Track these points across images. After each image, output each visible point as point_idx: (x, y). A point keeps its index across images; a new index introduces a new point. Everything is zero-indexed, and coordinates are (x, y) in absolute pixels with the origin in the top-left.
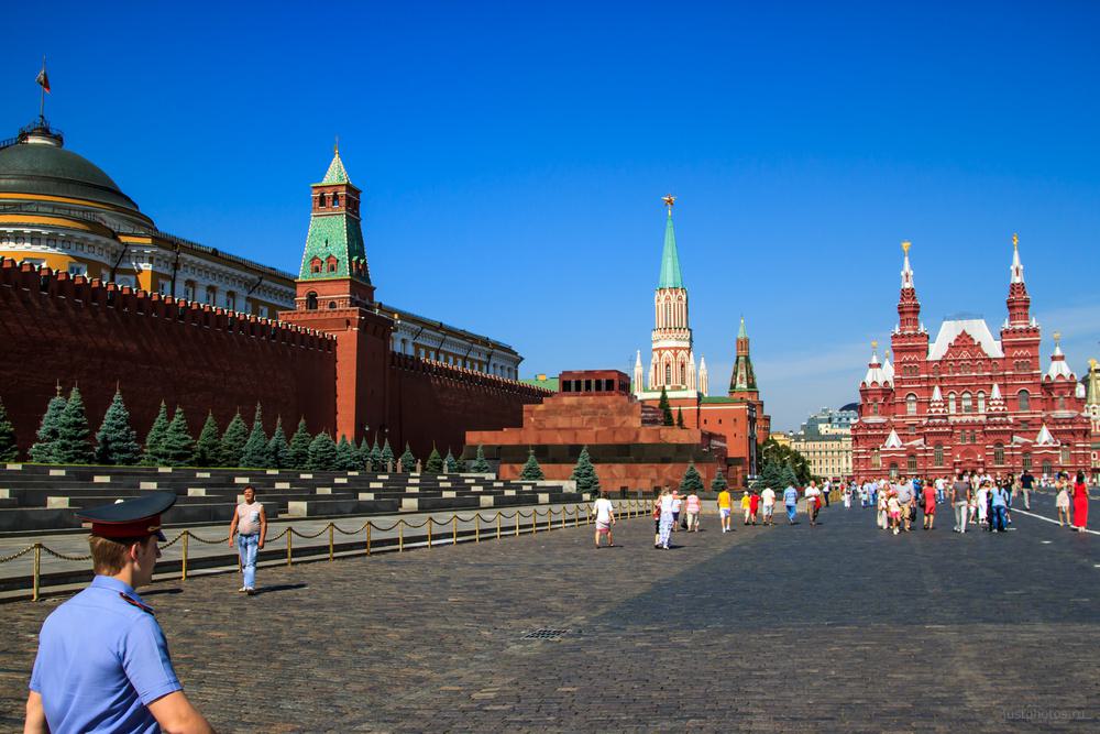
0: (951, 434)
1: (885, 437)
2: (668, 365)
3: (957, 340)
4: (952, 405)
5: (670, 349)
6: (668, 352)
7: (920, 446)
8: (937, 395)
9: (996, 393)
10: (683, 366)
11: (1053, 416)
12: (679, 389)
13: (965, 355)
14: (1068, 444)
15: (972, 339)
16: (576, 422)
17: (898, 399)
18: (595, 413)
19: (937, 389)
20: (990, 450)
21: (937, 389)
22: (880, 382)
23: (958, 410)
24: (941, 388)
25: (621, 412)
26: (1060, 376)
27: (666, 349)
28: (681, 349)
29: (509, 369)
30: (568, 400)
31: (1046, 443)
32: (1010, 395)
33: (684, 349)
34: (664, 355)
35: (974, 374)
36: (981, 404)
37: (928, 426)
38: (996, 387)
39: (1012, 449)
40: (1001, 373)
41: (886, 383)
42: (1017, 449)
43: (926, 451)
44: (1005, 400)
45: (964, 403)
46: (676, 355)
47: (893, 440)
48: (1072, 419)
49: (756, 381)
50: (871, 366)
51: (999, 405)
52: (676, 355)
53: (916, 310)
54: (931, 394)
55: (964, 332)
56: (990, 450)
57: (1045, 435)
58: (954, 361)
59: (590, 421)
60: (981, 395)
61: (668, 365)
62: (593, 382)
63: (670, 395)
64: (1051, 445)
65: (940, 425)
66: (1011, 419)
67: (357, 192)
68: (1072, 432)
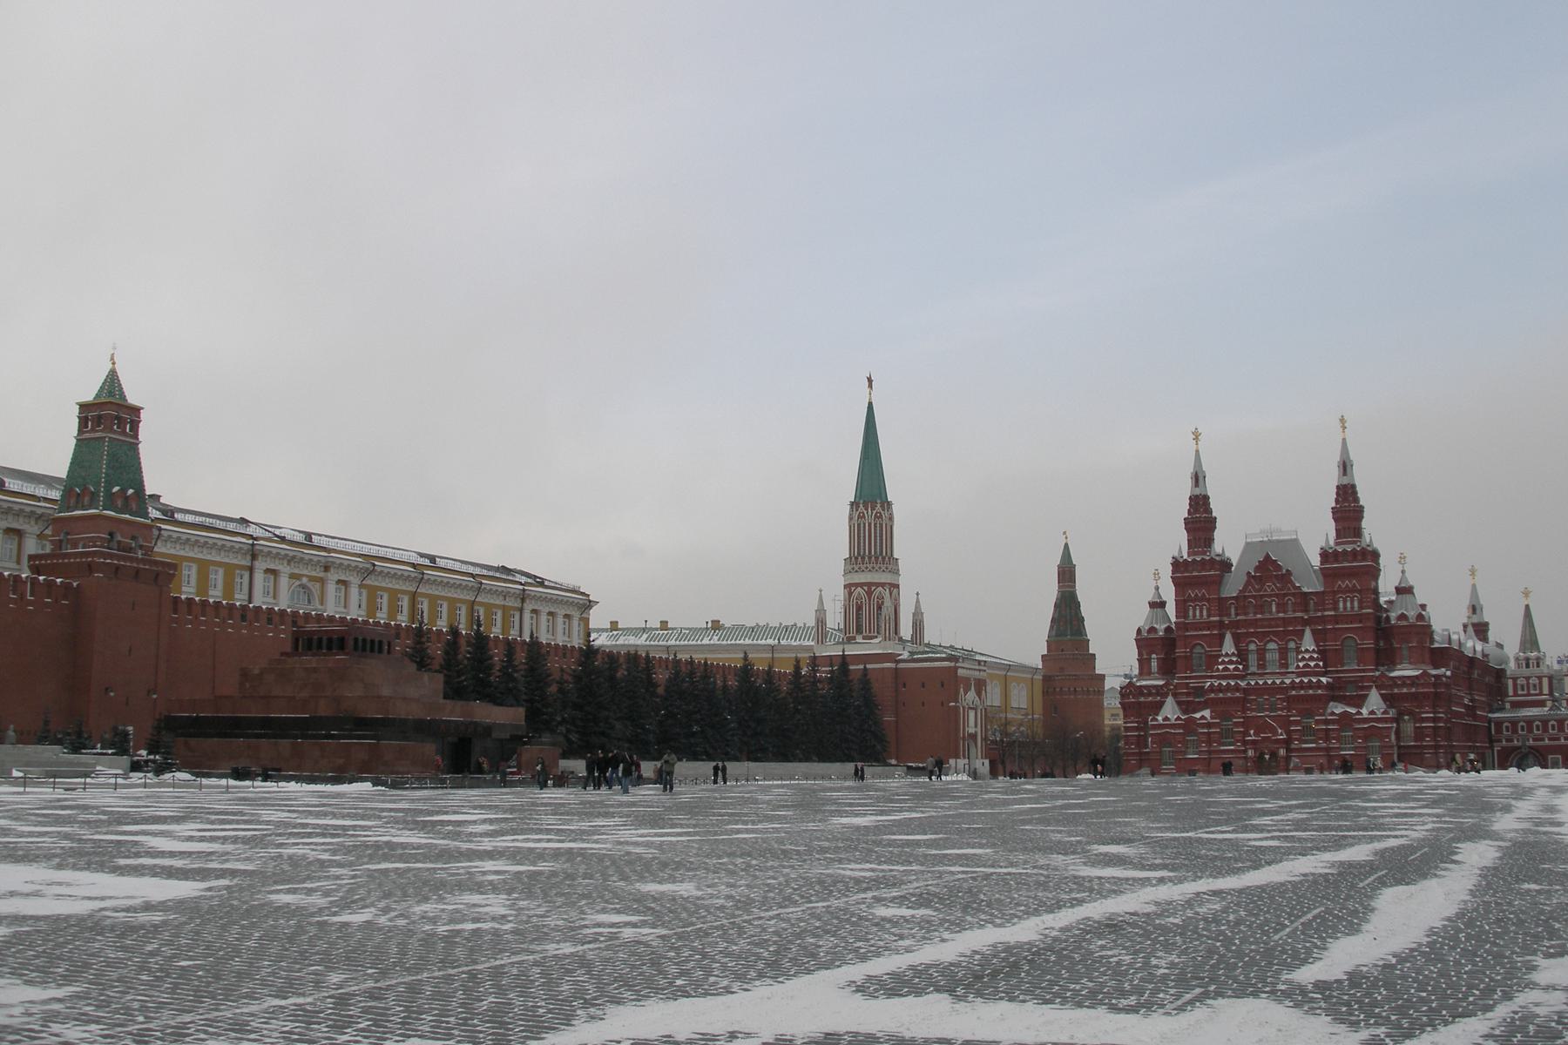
0: (1245, 700)
2: (859, 608)
3: (1257, 569)
4: (1253, 659)
5: (861, 585)
7: (1203, 717)
8: (1229, 646)
9: (1308, 643)
10: (880, 608)
13: (1269, 587)
14: (1410, 713)
15: (1279, 568)
17: (1180, 651)
19: (1228, 638)
20: (1297, 723)
21: (1228, 638)
22: (1161, 628)
24: (1237, 639)
27: (857, 585)
28: (878, 585)
29: (567, 616)
31: (1372, 712)
32: (1331, 645)
33: (883, 585)
34: (855, 594)
36: (1292, 655)
38: (1308, 634)
39: (1327, 722)
41: (1168, 629)
42: (1333, 722)
43: (1209, 725)
44: (1323, 654)
46: (869, 593)
47: (1170, 711)
48: (1416, 677)
50: (1153, 605)
51: (1311, 659)
52: (869, 593)
53: (1210, 524)
54: (1221, 645)
56: (1297, 723)
57: (1374, 703)
58: (1254, 597)
60: (1292, 645)
61: (859, 608)
66: (1324, 680)
67: (136, 410)
68: (1414, 697)
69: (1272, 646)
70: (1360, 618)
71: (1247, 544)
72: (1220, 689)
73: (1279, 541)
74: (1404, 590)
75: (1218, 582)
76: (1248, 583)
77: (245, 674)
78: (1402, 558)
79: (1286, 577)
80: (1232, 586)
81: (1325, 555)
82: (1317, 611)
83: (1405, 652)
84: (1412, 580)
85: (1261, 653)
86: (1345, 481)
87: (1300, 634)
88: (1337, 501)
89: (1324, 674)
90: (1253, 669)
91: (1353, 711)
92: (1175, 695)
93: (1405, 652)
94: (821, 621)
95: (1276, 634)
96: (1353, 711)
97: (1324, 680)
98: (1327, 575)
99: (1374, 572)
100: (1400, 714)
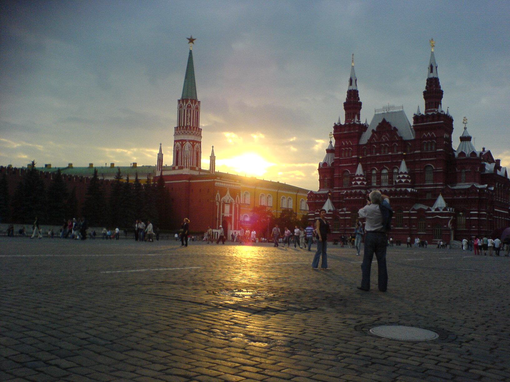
1: (324, 203)
3: (378, 127)
8: (360, 171)
9: (403, 168)
11: (455, 188)
23: (377, 183)
24: (365, 168)
26: (462, 154)
31: (437, 209)
34: (176, 146)
35: (390, 153)
37: (347, 195)
39: (410, 215)
40: (412, 153)
43: (346, 215)
45: (383, 177)
48: (468, 189)
51: (404, 178)
52: (182, 145)
54: (355, 171)
55: (384, 121)
57: (441, 202)
64: (441, 211)
65: (355, 194)
66: (409, 190)
69: (385, 171)
70: (436, 154)
71: (375, 115)
72: (351, 195)
73: (392, 113)
74: (465, 139)
75: (359, 136)
76: (373, 136)
78: (465, 119)
79: (394, 131)
80: (365, 138)
81: (417, 118)
82: (411, 151)
83: (464, 176)
84: (470, 133)
85: (379, 175)
86: (432, 75)
87: (399, 164)
88: (426, 88)
89: (409, 187)
90: (375, 184)
91: (426, 208)
92: (332, 199)
93: (464, 176)
94: (160, 160)
95: (387, 164)
96: (426, 208)
97: (409, 190)
98: (417, 129)
99: (450, 129)
100: (457, 211)
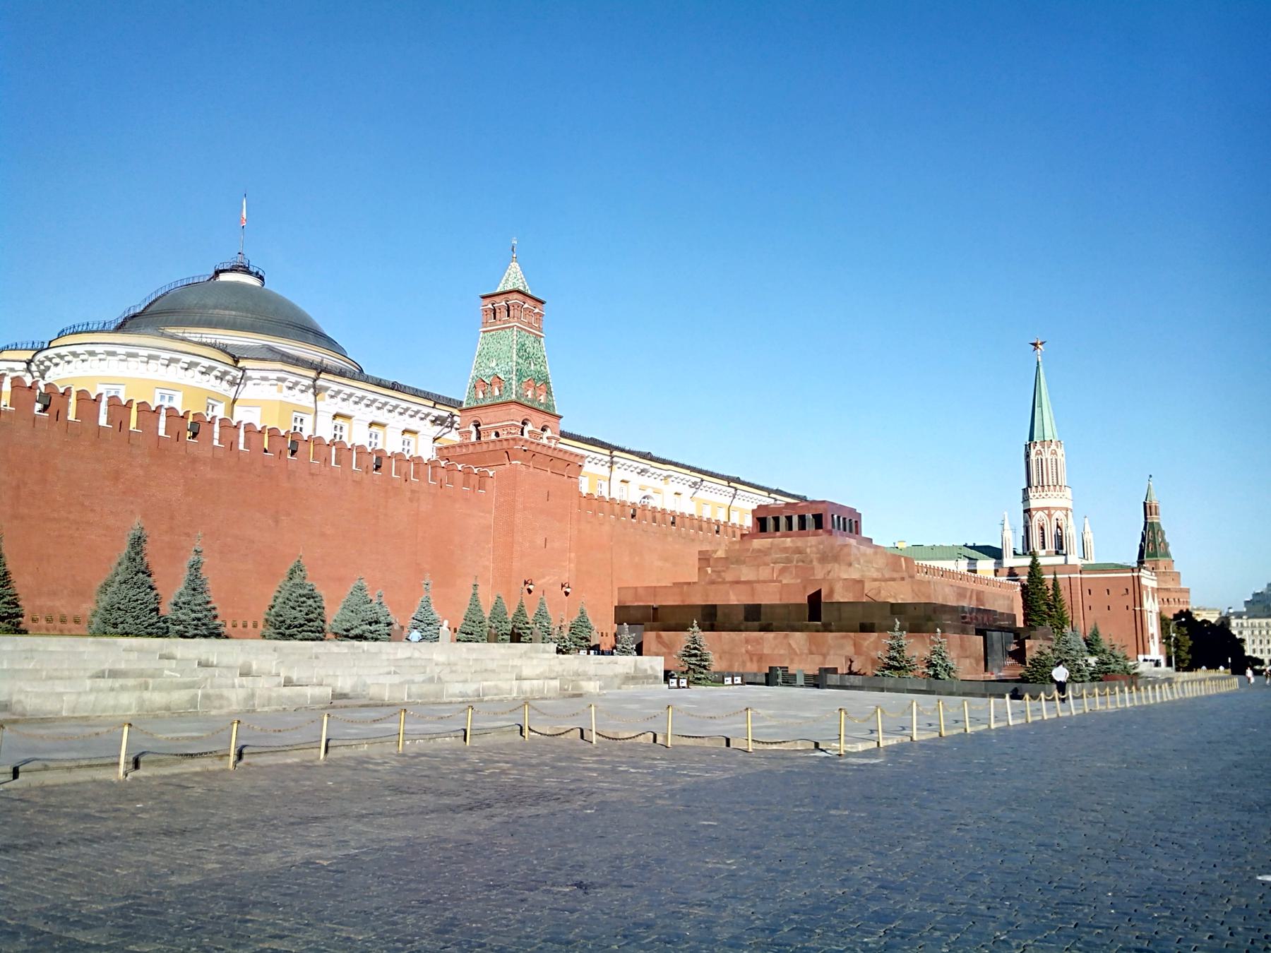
2: (1042, 529)
5: (1042, 509)
6: (1040, 513)
12: (1057, 553)
16: (764, 573)
18: (789, 560)
25: (824, 559)
28: (1056, 509)
30: (759, 543)
33: (1061, 509)
46: (1049, 516)
49: (1170, 549)
52: (1049, 516)
59: (782, 571)
62: (795, 519)
63: (1042, 561)
77: (705, 559)
